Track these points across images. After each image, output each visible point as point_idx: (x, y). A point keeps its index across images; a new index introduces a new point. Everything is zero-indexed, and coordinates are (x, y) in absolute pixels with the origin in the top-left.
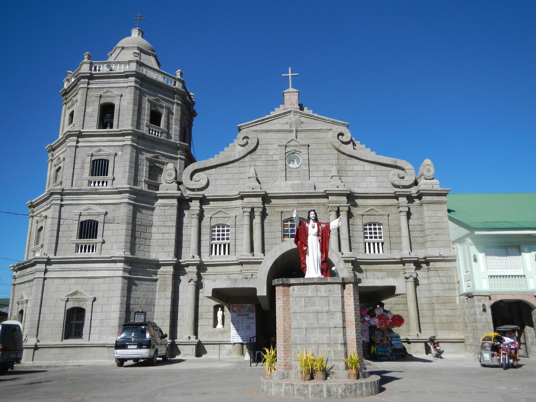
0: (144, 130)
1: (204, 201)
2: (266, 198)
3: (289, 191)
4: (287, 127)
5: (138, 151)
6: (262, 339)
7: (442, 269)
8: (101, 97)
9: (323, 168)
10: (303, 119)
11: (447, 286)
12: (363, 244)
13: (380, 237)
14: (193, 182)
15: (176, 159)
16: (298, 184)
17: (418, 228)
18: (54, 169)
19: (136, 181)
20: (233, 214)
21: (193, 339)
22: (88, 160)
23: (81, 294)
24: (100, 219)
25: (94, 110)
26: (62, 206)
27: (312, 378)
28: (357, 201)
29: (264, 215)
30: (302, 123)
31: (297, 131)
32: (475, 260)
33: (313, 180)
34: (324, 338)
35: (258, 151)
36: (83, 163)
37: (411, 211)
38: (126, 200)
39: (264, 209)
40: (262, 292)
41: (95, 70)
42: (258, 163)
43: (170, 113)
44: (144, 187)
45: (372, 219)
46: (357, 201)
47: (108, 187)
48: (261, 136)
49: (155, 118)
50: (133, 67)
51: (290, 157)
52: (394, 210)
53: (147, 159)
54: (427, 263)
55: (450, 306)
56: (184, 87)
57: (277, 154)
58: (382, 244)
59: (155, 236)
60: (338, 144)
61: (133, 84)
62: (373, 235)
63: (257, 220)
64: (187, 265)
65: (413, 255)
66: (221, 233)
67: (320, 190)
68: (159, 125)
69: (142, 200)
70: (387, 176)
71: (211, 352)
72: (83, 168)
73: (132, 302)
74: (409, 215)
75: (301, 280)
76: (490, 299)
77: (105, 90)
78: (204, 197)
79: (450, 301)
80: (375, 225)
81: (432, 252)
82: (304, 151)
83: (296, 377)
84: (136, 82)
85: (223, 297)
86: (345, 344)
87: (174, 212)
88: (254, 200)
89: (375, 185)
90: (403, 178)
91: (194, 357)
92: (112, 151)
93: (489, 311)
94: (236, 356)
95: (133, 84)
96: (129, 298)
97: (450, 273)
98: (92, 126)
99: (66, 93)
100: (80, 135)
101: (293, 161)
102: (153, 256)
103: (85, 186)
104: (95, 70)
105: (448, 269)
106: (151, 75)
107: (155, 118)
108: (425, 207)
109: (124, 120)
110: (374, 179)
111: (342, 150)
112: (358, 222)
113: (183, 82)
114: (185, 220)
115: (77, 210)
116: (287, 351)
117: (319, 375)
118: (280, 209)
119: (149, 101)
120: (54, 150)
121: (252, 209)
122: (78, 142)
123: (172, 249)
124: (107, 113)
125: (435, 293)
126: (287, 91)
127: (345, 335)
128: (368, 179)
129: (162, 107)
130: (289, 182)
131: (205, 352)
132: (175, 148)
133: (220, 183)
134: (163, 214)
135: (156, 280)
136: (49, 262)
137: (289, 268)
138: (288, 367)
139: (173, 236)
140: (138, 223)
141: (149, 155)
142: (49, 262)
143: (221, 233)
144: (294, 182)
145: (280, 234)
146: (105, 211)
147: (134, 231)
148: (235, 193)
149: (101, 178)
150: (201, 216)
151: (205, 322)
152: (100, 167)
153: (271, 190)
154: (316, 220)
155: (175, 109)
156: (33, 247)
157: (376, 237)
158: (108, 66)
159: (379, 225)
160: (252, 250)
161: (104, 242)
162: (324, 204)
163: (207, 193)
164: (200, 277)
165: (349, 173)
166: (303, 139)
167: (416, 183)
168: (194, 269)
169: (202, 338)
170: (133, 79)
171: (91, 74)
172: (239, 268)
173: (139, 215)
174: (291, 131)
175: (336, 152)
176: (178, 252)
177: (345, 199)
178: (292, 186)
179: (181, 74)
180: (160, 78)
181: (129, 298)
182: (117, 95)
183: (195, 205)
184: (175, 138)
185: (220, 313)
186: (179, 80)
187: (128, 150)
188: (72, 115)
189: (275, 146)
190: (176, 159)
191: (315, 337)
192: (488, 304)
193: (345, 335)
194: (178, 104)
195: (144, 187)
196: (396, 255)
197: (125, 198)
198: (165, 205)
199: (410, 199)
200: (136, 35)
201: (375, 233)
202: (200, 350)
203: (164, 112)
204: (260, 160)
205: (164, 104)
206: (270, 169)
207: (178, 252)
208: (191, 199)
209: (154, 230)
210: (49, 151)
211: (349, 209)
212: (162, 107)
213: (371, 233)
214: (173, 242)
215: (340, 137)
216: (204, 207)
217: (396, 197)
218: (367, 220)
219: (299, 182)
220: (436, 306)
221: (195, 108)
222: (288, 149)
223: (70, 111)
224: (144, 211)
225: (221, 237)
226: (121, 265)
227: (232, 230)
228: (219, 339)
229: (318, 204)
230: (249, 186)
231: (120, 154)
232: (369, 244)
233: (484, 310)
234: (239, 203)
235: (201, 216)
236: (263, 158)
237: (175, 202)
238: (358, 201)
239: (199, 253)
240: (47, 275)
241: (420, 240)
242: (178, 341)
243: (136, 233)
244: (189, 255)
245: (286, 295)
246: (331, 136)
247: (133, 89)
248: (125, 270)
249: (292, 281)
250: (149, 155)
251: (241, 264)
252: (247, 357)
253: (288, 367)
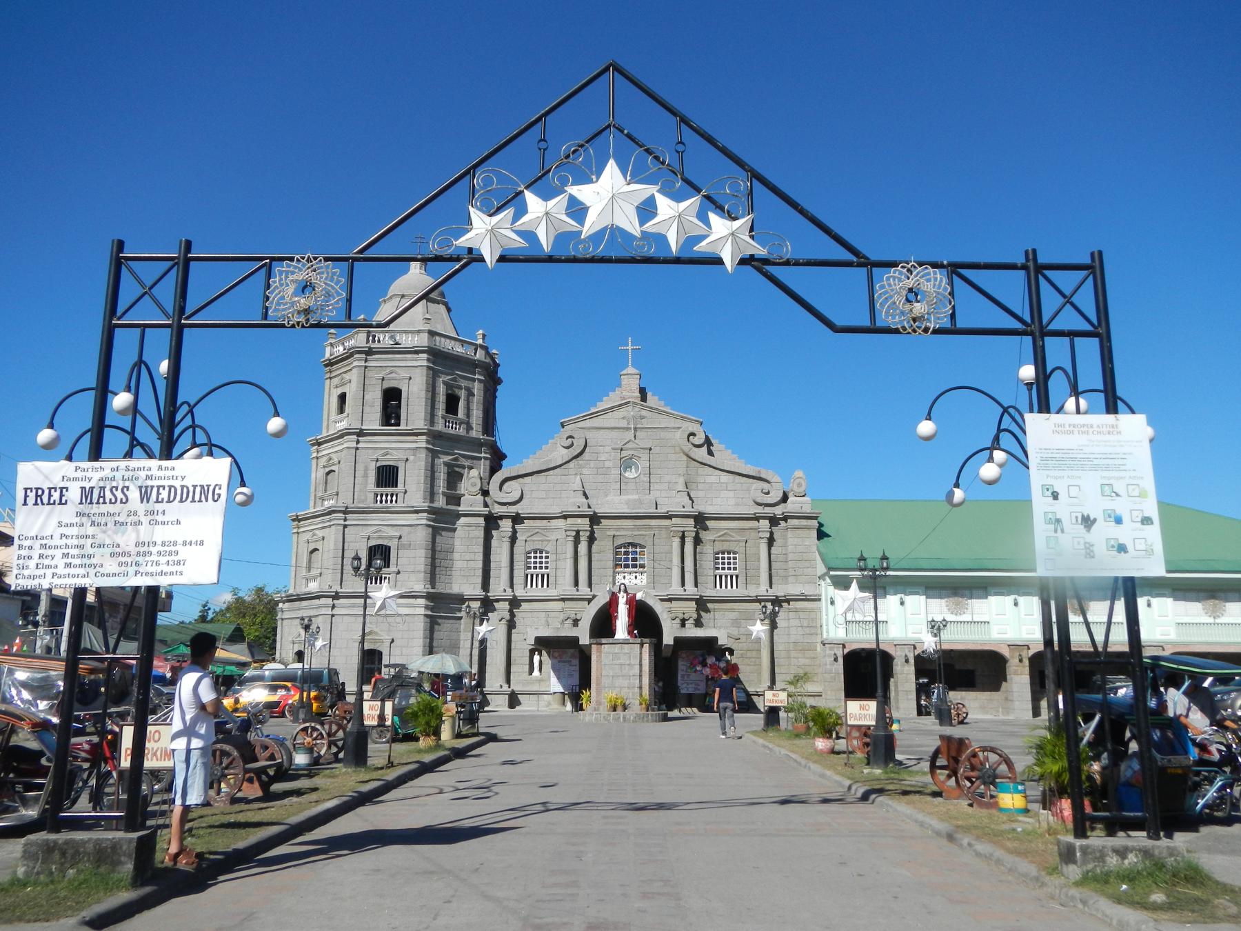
0: (439, 426)
1: (517, 519)
2: (595, 519)
3: (624, 509)
4: (623, 424)
5: (434, 454)
6: (579, 686)
7: (803, 610)
8: (383, 379)
9: (667, 478)
10: (644, 413)
11: (807, 630)
13: (735, 569)
14: (502, 494)
15: (480, 458)
16: (635, 500)
17: (781, 558)
18: (322, 472)
19: (432, 495)
20: (553, 537)
21: (505, 687)
22: (373, 467)
23: (376, 633)
24: (393, 544)
25: (375, 398)
26: (345, 526)
27: (615, 710)
28: (708, 523)
29: (592, 539)
30: (642, 418)
31: (635, 430)
32: (832, 603)
33: (655, 494)
34: (626, 683)
35: (586, 455)
36: (366, 469)
37: (775, 536)
38: (424, 522)
39: (592, 532)
40: (585, 640)
41: (374, 341)
42: (585, 471)
43: (470, 393)
44: (441, 502)
45: (726, 546)
46: (708, 523)
47: (400, 505)
48: (589, 435)
49: (452, 404)
50: (422, 341)
51: (627, 464)
52: (753, 534)
53: (446, 464)
54: (788, 601)
55: (810, 654)
56: (488, 353)
57: (609, 458)
59: (458, 564)
60: (687, 447)
61: (425, 363)
63: (583, 547)
64: (498, 600)
65: (771, 592)
67: (662, 510)
68: (456, 413)
69: (443, 520)
70: (748, 490)
71: (527, 706)
72: (366, 476)
73: (435, 644)
74: (771, 541)
75: (610, 640)
76: (844, 646)
77: (388, 370)
78: (518, 514)
79: (810, 648)
81: (793, 589)
82: (645, 456)
83: (604, 709)
84: (428, 360)
85: (543, 644)
86: (641, 688)
87: (480, 533)
88: (579, 520)
89: (732, 502)
90: (768, 493)
91: (507, 709)
92: (401, 455)
93: (841, 660)
94: (556, 707)
95: (425, 363)
96: (431, 639)
97: (813, 615)
98: (373, 421)
99: (330, 363)
100: (361, 433)
102: (456, 589)
103: (369, 502)
104: (374, 341)
105: (812, 610)
106: (447, 345)
107: (452, 404)
108: (790, 533)
109: (415, 413)
110: (731, 494)
111: (692, 455)
112: (707, 550)
113: (485, 348)
114: (494, 543)
115: (365, 532)
116: (599, 692)
117: (619, 708)
118: (612, 533)
119: (444, 383)
120: (319, 444)
121: (578, 532)
122: (358, 442)
123: (479, 580)
124: (392, 400)
125: (793, 638)
126: (624, 372)
127: (641, 681)
128: (724, 494)
129: (460, 388)
130: (623, 497)
131: (519, 703)
132: (476, 445)
133: (539, 497)
134: (467, 535)
135: (460, 618)
136: (336, 596)
137: (603, 625)
138: (599, 703)
139: (480, 564)
140: (438, 549)
141: (447, 458)
142: (336, 596)
144: (631, 497)
145: (611, 564)
146: (398, 534)
147: (433, 558)
148: (556, 510)
149: (389, 490)
150: (513, 539)
151: (519, 668)
152: (388, 476)
153: (601, 509)
154: (626, 591)
155: (477, 388)
156: (304, 573)
157: (729, 569)
158: (392, 337)
160: (576, 584)
161: (399, 573)
162: (667, 527)
163: (521, 509)
164: (512, 615)
165: (700, 486)
166: (644, 440)
167: (785, 499)
168: (506, 605)
169: (516, 687)
170: (425, 356)
171: (370, 348)
172: (561, 603)
173: (438, 539)
174: (628, 429)
175: (685, 458)
176: (486, 585)
177: (692, 521)
178: (628, 503)
179: (484, 336)
180: (459, 349)
181: (431, 639)
182: (404, 378)
183: (506, 525)
184: (477, 433)
185: (536, 658)
186: (481, 346)
187: (423, 455)
188: (342, 398)
189: (608, 449)
190: (480, 458)
191: (620, 682)
192: (840, 654)
193: (641, 681)
194: (480, 381)
195: (441, 502)
196: (752, 592)
197: (422, 519)
198: (469, 525)
199: (774, 521)
200: (418, 271)
202: (514, 701)
203: (463, 394)
205: (464, 383)
206: (600, 478)
207: (486, 585)
208: (501, 518)
209: (456, 556)
210: (313, 445)
211: (697, 533)
212: (460, 388)
214: (480, 572)
216: (517, 527)
217: (757, 519)
218: (719, 546)
219: (636, 497)
220: (793, 654)
221: (501, 373)
222: (624, 453)
223: (340, 391)
224: (443, 533)
226: (422, 601)
227: (552, 557)
228: (535, 688)
229: (660, 527)
230: (573, 502)
231: (411, 455)
233: (836, 660)
234: (561, 522)
235: (513, 539)
236: (592, 464)
237: (481, 521)
238: (710, 523)
239: (512, 586)
240: (335, 612)
241: (782, 573)
242: (487, 689)
243: (436, 564)
244: (499, 587)
245: (599, 651)
246: (679, 437)
247: (424, 370)
248: (427, 607)
249: (604, 640)
250: (447, 458)
251: (563, 600)
252: (569, 707)
253: (599, 703)
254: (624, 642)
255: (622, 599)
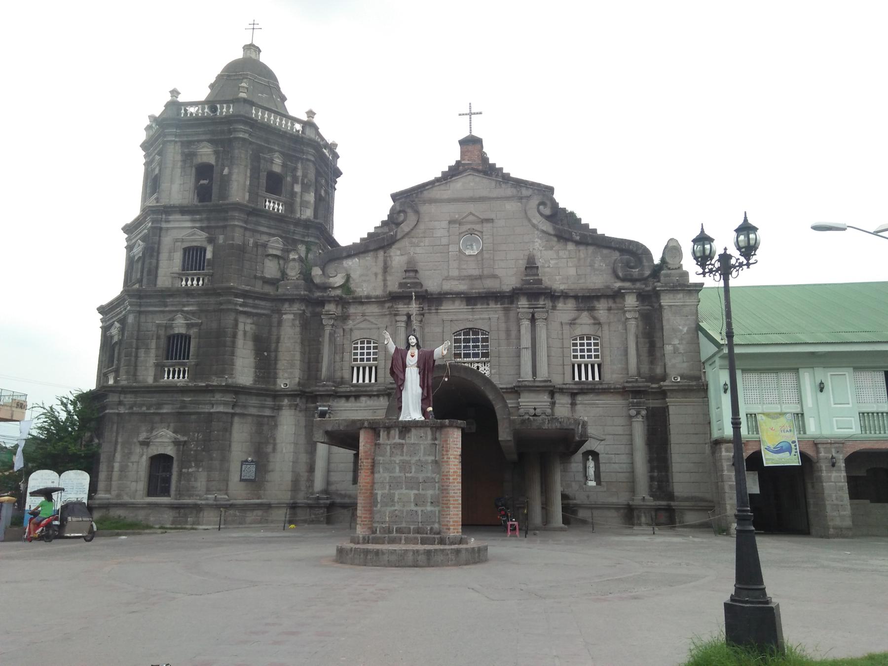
12: (570, 368)
58: (599, 366)
62: (586, 354)
66: (365, 351)
80: (589, 339)
101: (472, 245)
143: (365, 351)
157: (589, 357)
159: (594, 339)
201: (589, 350)
204: (422, 244)
213: (582, 351)
215: (541, 207)
225: (365, 357)
232: (579, 366)
254: (415, 424)
255: (412, 359)
